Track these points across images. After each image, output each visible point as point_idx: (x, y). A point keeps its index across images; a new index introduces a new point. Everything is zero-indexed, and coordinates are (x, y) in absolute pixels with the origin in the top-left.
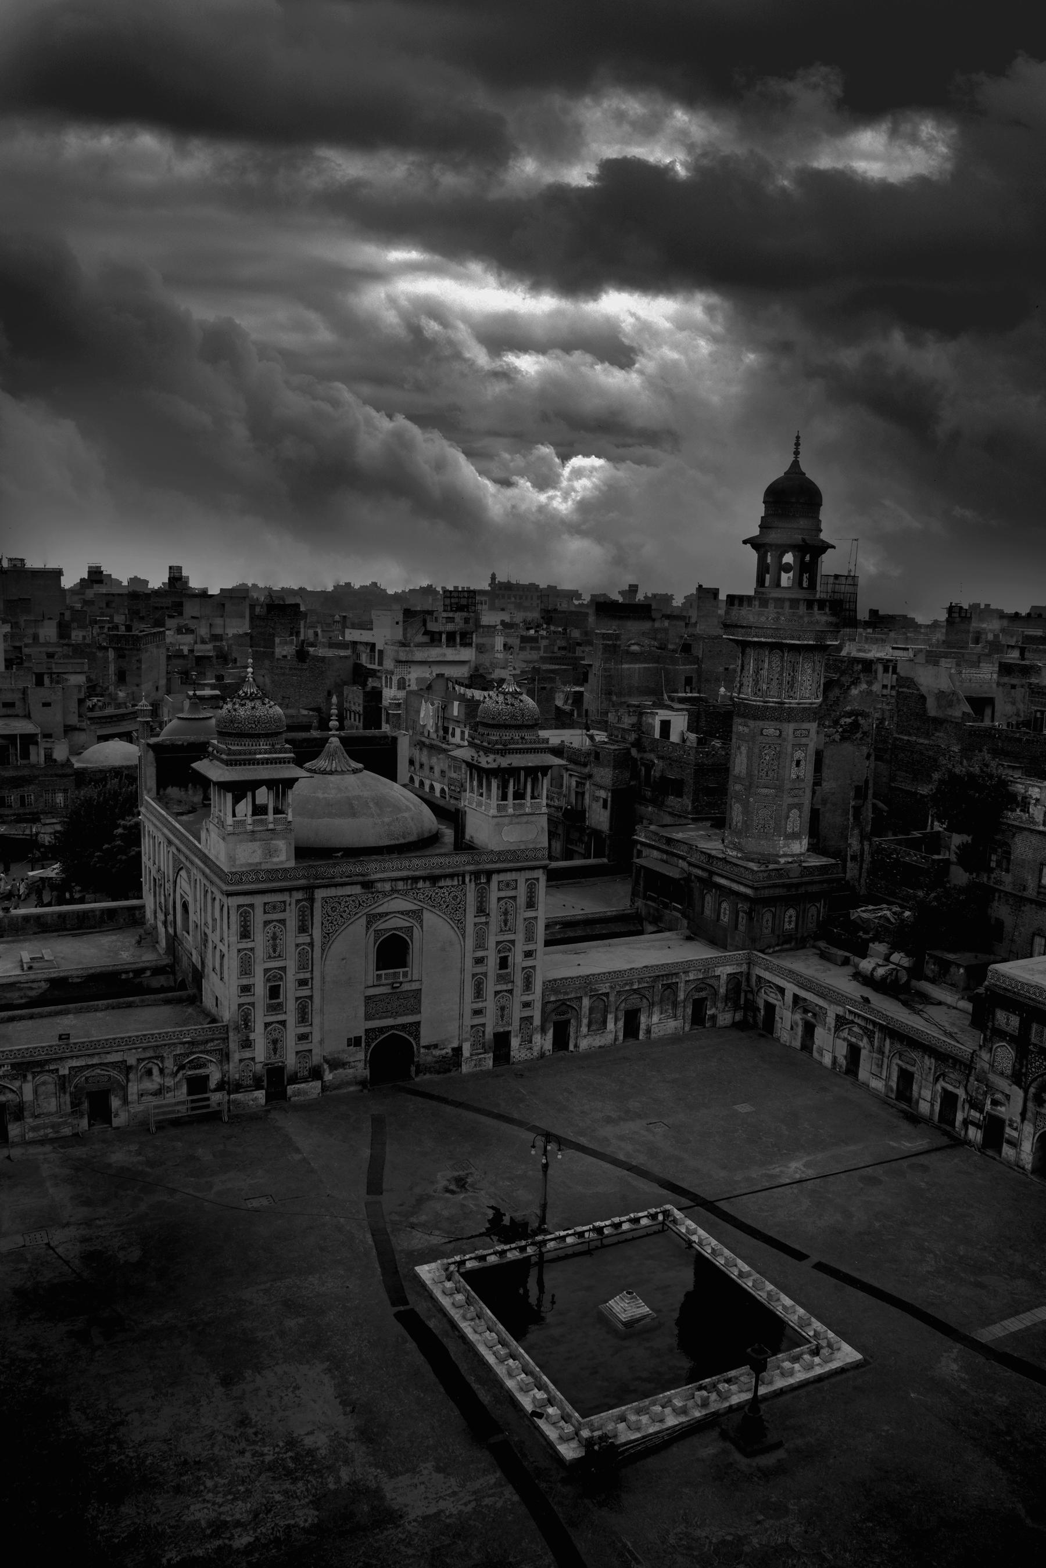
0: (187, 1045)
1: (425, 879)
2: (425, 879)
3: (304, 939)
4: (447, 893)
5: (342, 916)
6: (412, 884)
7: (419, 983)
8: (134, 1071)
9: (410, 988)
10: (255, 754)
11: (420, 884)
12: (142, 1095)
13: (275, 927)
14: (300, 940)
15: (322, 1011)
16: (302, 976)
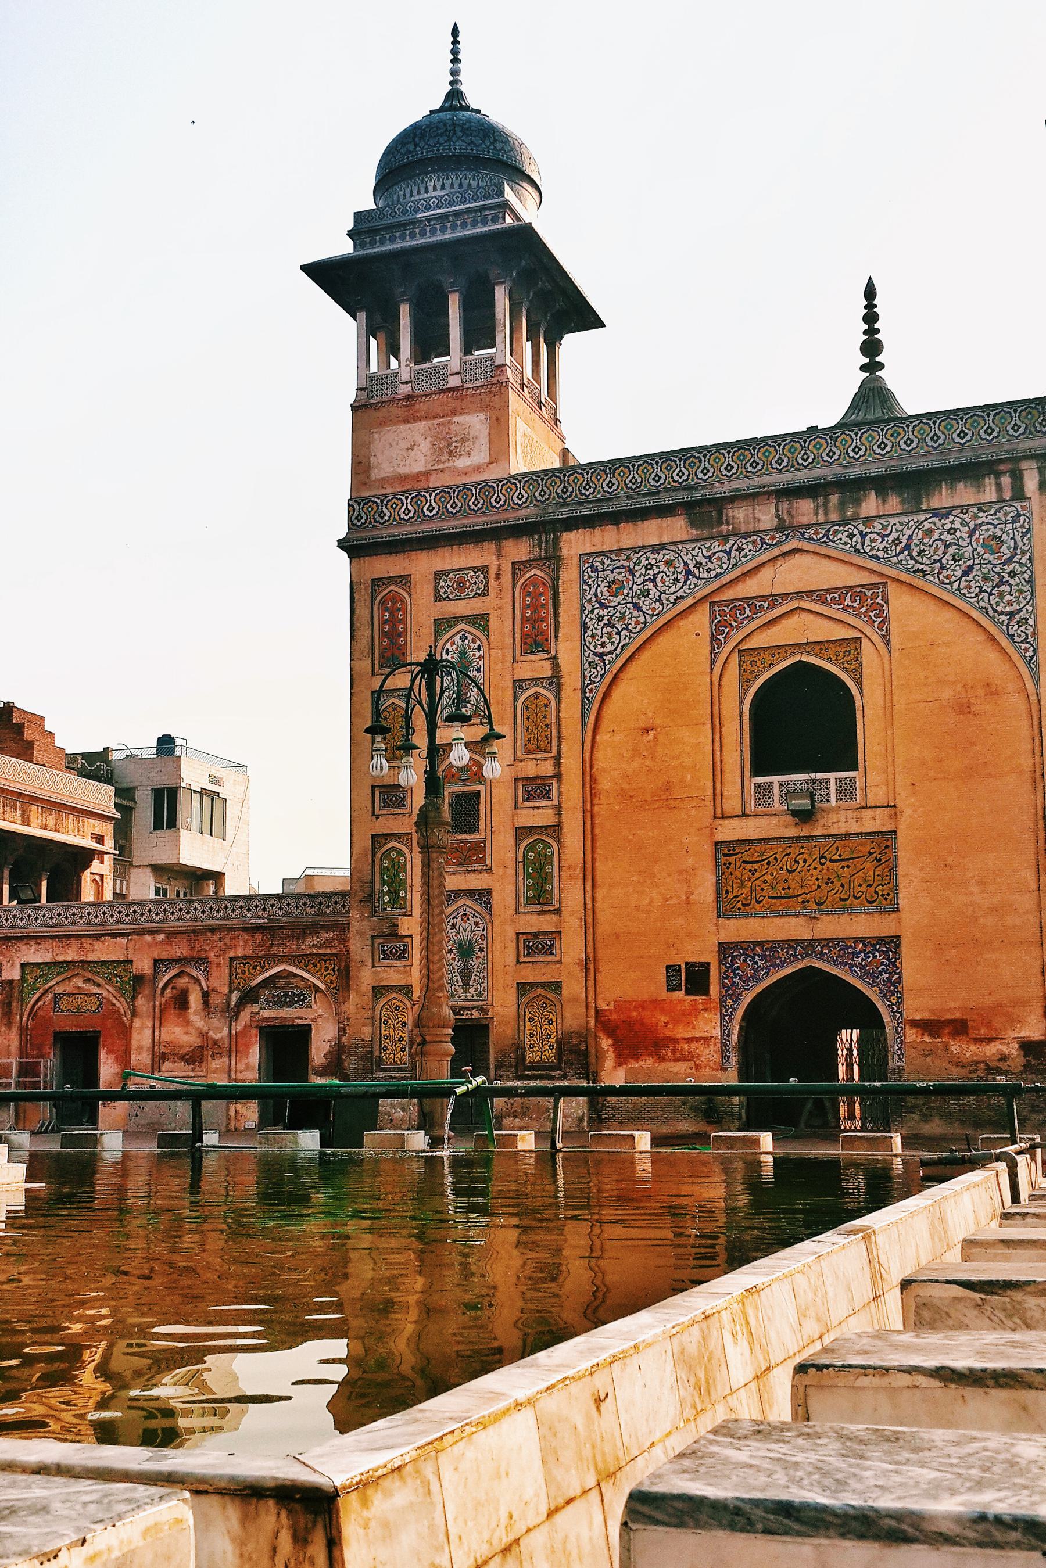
0: (258, 937)
1: (882, 484)
2: (882, 484)
3: (537, 666)
4: (963, 532)
5: (637, 607)
6: (842, 506)
7: (887, 811)
8: (147, 992)
9: (855, 828)
10: (417, 211)
11: (870, 505)
12: (163, 1057)
13: (464, 638)
14: (524, 671)
15: (589, 874)
16: (530, 769)
